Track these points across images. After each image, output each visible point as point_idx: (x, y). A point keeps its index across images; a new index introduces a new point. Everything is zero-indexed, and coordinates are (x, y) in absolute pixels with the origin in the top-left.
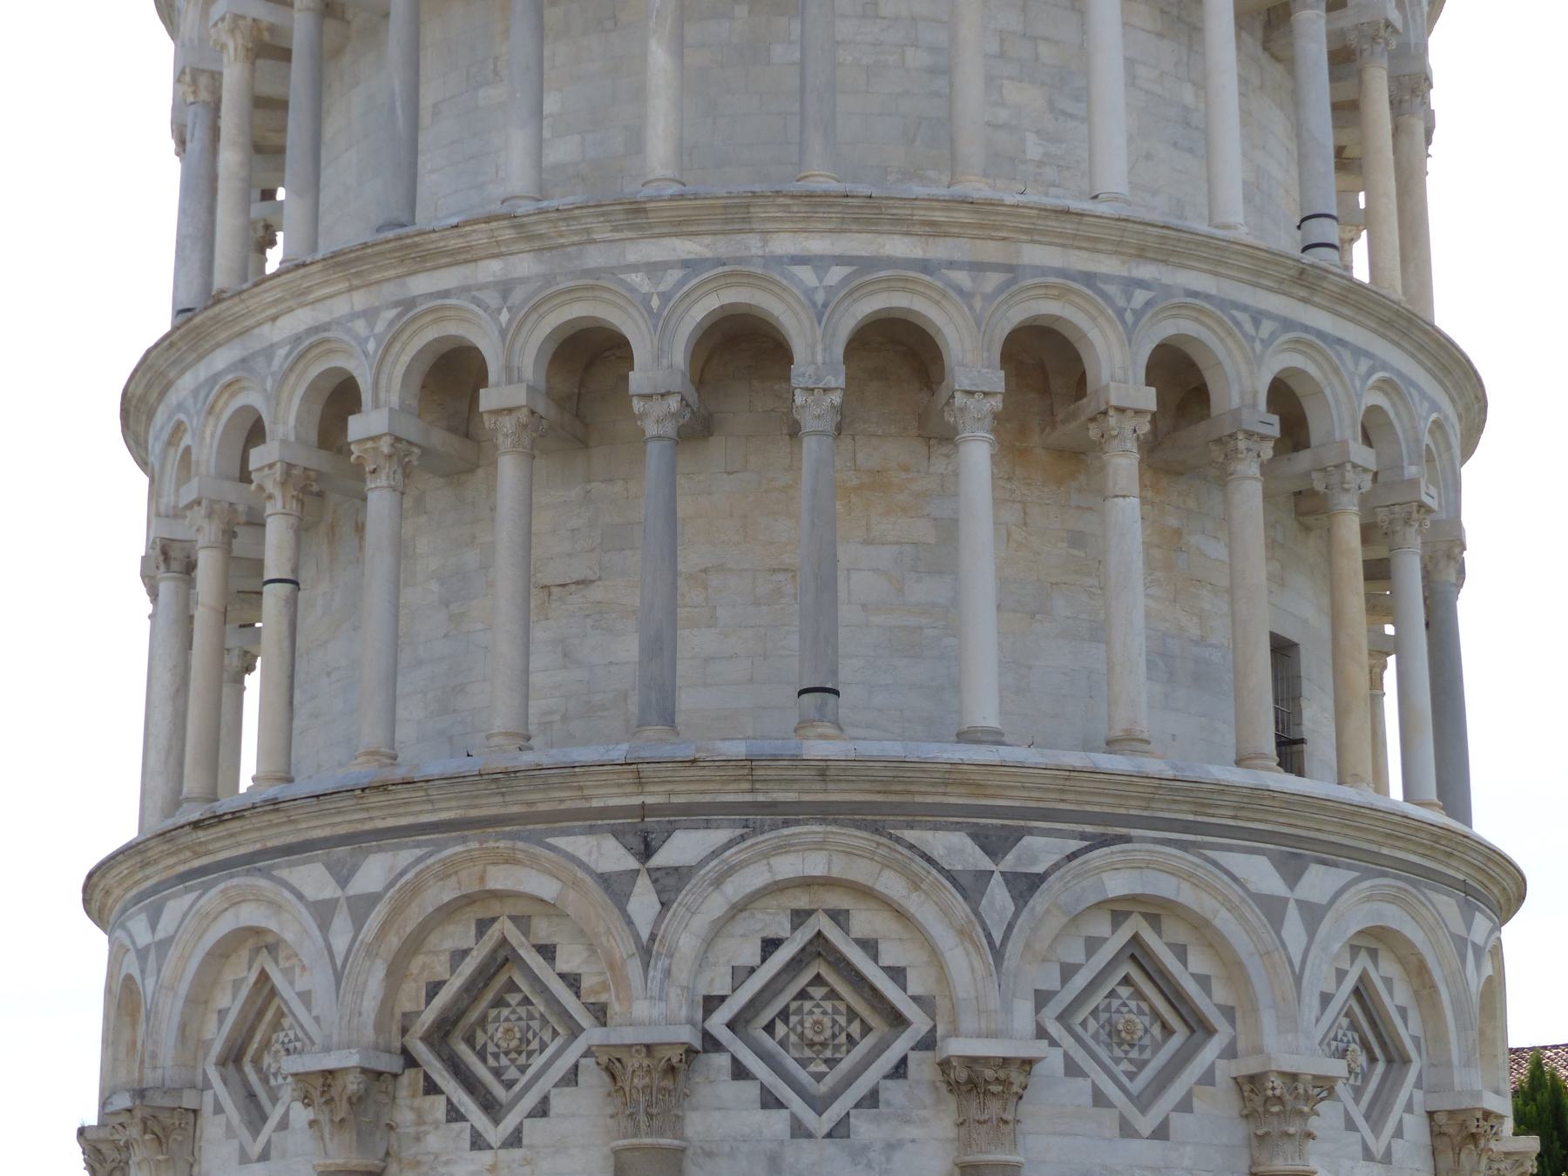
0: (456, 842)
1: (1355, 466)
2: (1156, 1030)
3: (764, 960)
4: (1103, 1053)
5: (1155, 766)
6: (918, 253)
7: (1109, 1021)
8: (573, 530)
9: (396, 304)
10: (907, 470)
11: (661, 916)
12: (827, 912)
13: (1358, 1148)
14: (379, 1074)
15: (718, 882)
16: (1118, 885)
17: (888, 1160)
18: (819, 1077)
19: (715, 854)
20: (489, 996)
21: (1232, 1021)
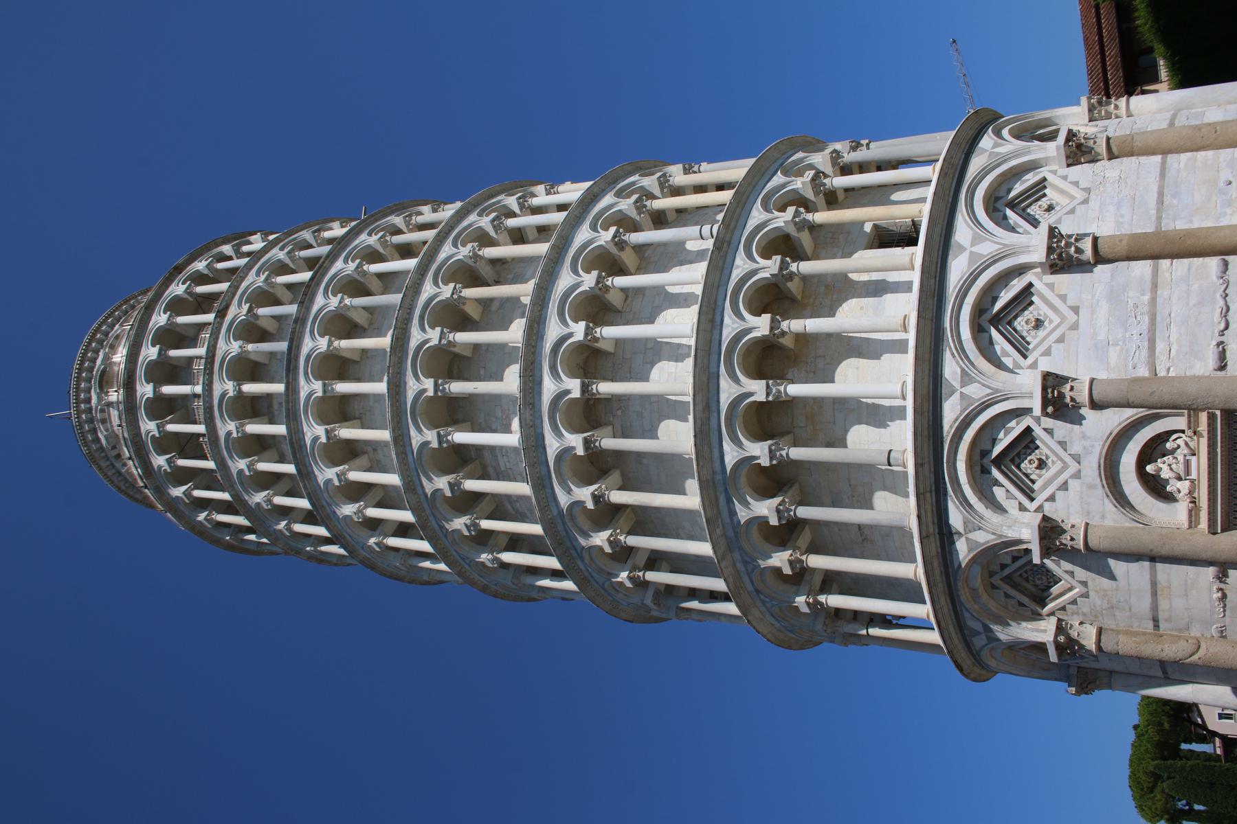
3: (1004, 486)
7: (1028, 331)
8: (839, 530)
9: (758, 594)
10: (805, 406)
11: (984, 530)
12: (981, 459)
13: (1083, 206)
15: (970, 506)
17: (1089, 438)
18: (1053, 462)
19: (958, 508)
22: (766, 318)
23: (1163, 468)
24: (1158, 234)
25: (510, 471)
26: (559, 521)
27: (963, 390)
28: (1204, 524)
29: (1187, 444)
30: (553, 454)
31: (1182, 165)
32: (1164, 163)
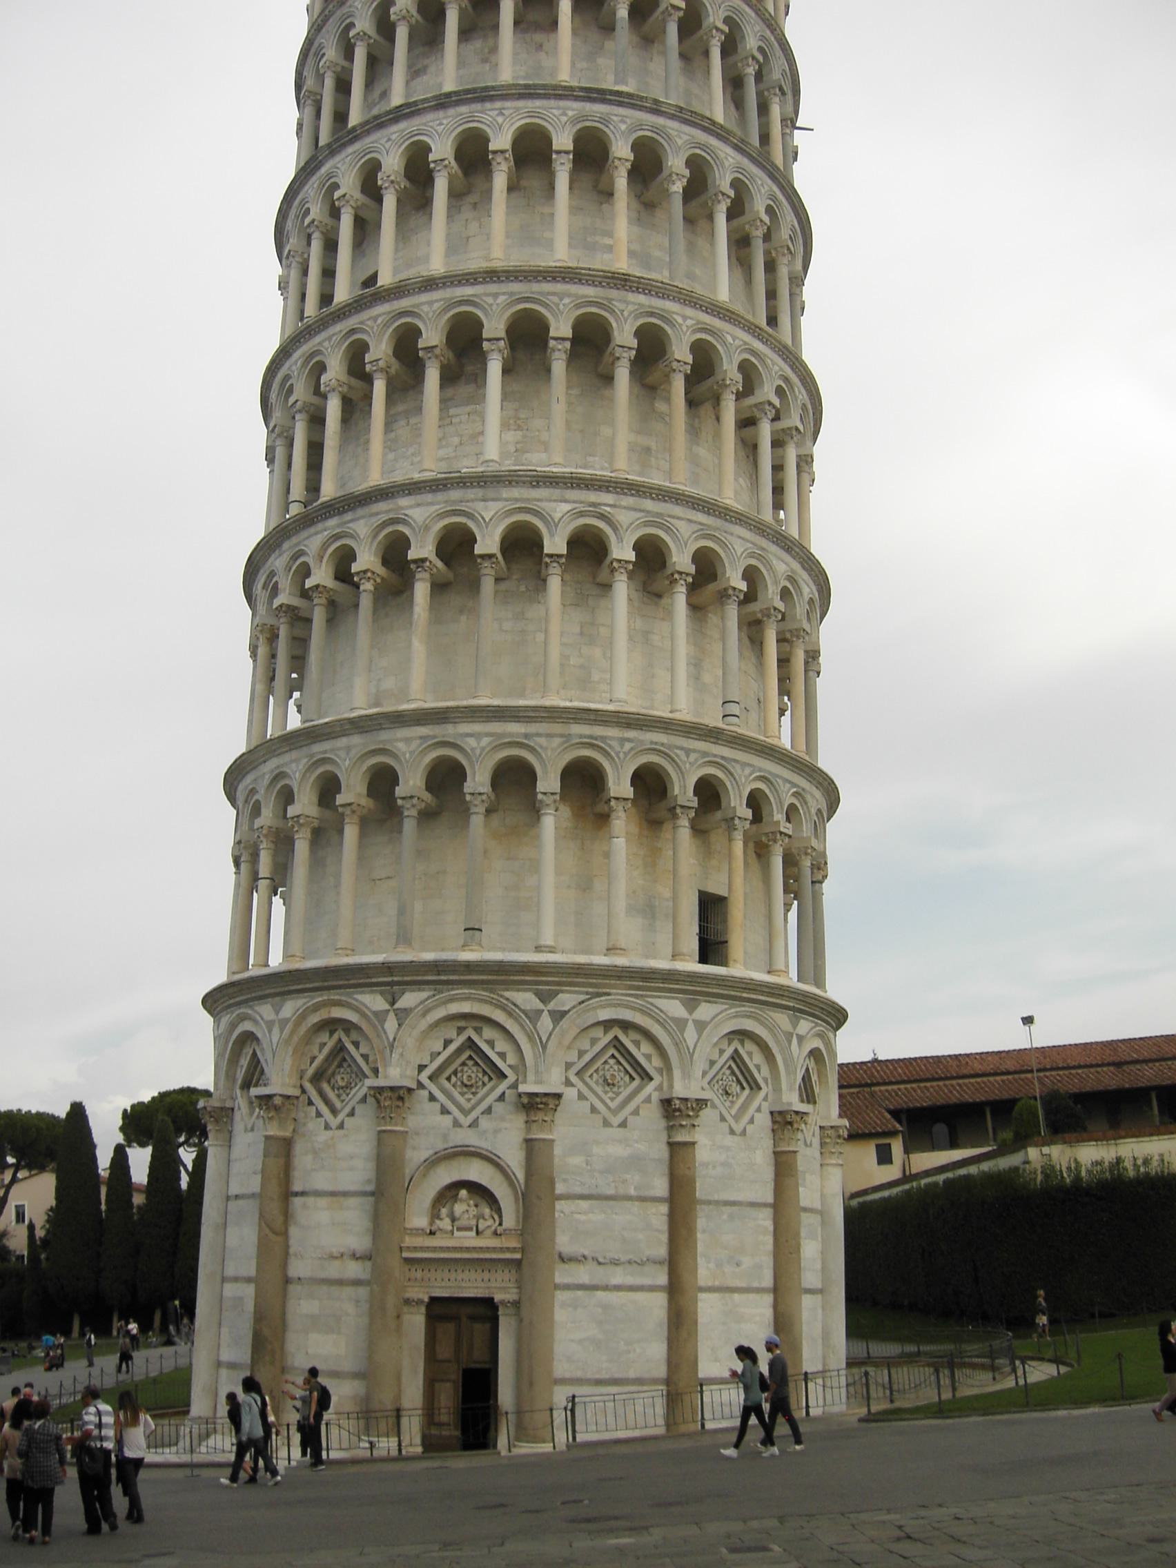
0: (319, 996)
1: (740, 818)
2: (627, 1078)
3: (444, 1049)
4: (599, 1090)
5: (621, 961)
6: (523, 731)
11: (398, 1030)
13: (727, 1130)
14: (288, 1097)
15: (424, 1015)
16: (604, 1015)
18: (469, 1100)
19: (422, 1003)
20: (336, 1063)
21: (662, 1075)
22: (629, 792)
23: (464, 1206)
24: (693, 1201)
25: (448, 421)
26: (391, 506)
27: (546, 1013)
28: (409, 1241)
29: (489, 1227)
30: (474, 510)
31: (761, 1222)
32: (765, 1205)
